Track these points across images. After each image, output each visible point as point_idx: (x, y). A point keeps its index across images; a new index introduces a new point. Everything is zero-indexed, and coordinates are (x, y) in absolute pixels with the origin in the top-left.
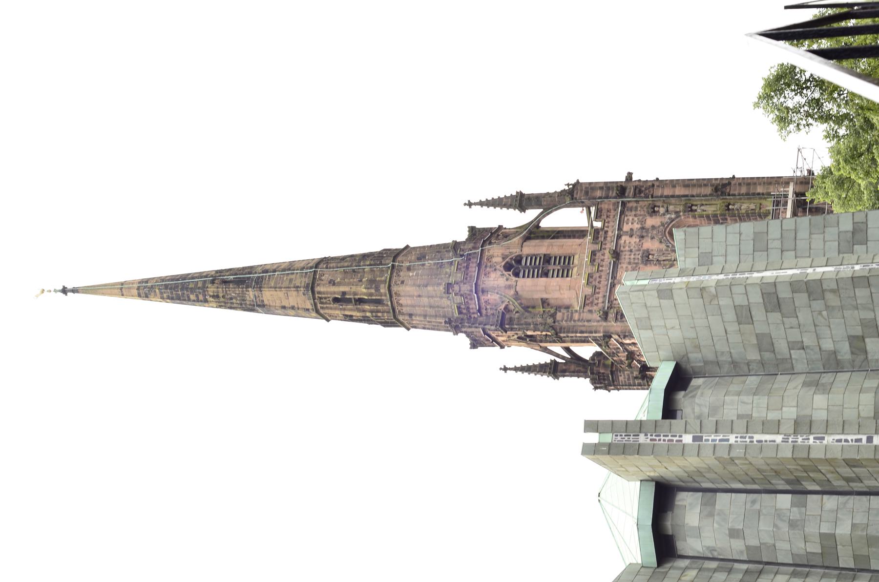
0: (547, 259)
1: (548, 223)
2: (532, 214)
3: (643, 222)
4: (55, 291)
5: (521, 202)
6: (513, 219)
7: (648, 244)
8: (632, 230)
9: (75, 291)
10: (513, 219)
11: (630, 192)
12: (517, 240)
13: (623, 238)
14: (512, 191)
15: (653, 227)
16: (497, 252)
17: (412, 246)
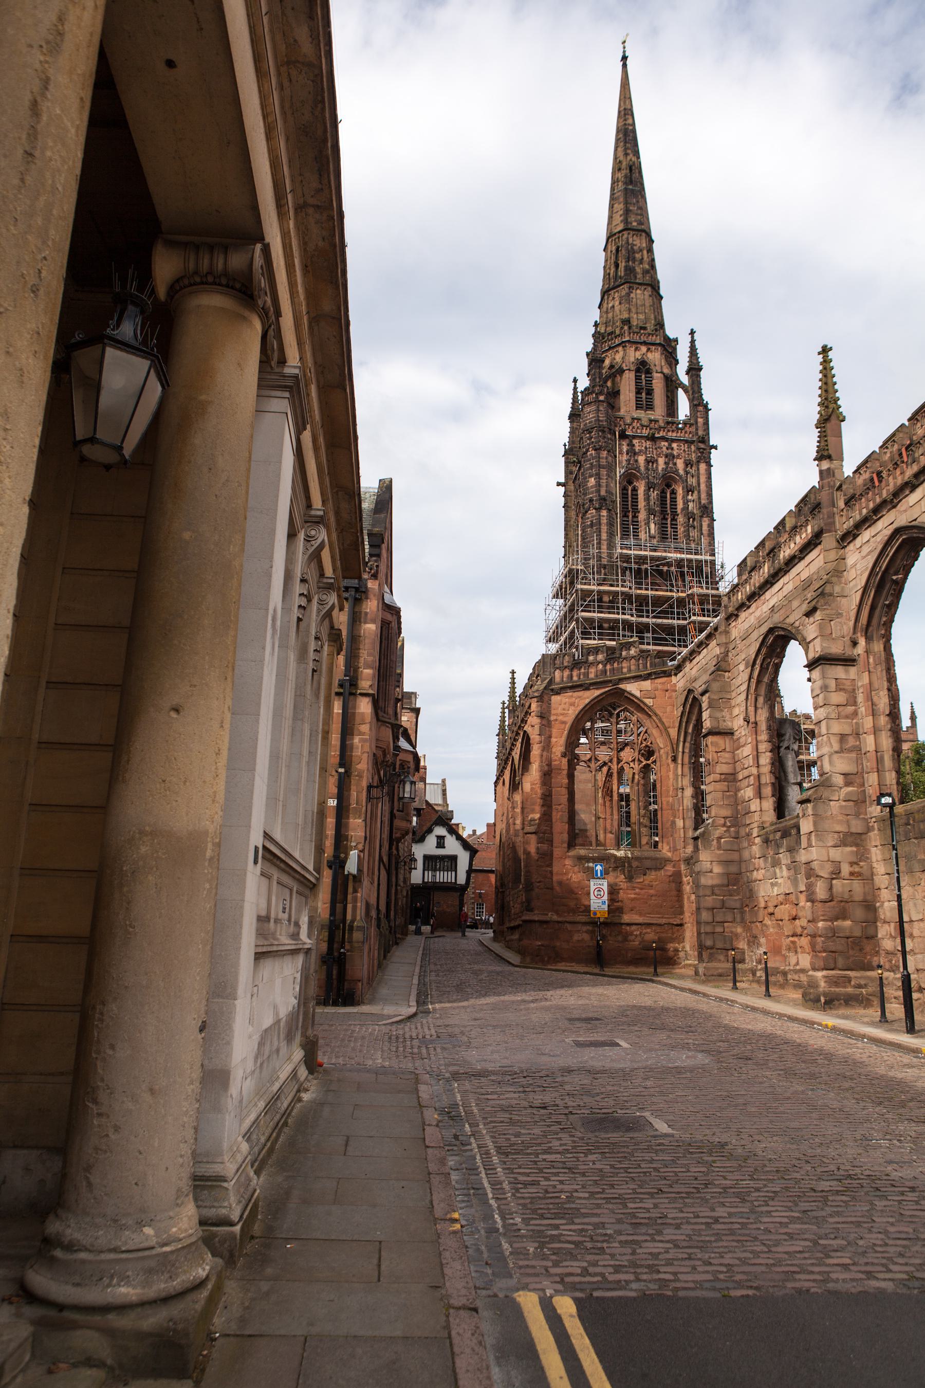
0: (650, 392)
1: (681, 392)
2: (684, 379)
3: (678, 457)
4: (624, 52)
5: (695, 369)
6: (682, 370)
7: (661, 461)
8: (672, 449)
9: (625, 66)
10: (682, 370)
11: (702, 446)
12: (666, 371)
13: (666, 444)
14: (702, 361)
15: (675, 464)
16: (655, 357)
17: (663, 302)
